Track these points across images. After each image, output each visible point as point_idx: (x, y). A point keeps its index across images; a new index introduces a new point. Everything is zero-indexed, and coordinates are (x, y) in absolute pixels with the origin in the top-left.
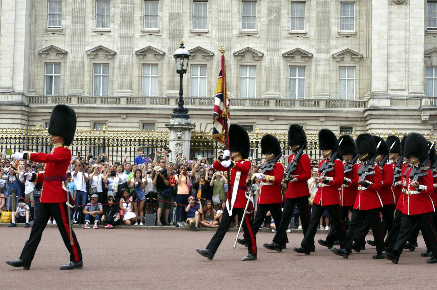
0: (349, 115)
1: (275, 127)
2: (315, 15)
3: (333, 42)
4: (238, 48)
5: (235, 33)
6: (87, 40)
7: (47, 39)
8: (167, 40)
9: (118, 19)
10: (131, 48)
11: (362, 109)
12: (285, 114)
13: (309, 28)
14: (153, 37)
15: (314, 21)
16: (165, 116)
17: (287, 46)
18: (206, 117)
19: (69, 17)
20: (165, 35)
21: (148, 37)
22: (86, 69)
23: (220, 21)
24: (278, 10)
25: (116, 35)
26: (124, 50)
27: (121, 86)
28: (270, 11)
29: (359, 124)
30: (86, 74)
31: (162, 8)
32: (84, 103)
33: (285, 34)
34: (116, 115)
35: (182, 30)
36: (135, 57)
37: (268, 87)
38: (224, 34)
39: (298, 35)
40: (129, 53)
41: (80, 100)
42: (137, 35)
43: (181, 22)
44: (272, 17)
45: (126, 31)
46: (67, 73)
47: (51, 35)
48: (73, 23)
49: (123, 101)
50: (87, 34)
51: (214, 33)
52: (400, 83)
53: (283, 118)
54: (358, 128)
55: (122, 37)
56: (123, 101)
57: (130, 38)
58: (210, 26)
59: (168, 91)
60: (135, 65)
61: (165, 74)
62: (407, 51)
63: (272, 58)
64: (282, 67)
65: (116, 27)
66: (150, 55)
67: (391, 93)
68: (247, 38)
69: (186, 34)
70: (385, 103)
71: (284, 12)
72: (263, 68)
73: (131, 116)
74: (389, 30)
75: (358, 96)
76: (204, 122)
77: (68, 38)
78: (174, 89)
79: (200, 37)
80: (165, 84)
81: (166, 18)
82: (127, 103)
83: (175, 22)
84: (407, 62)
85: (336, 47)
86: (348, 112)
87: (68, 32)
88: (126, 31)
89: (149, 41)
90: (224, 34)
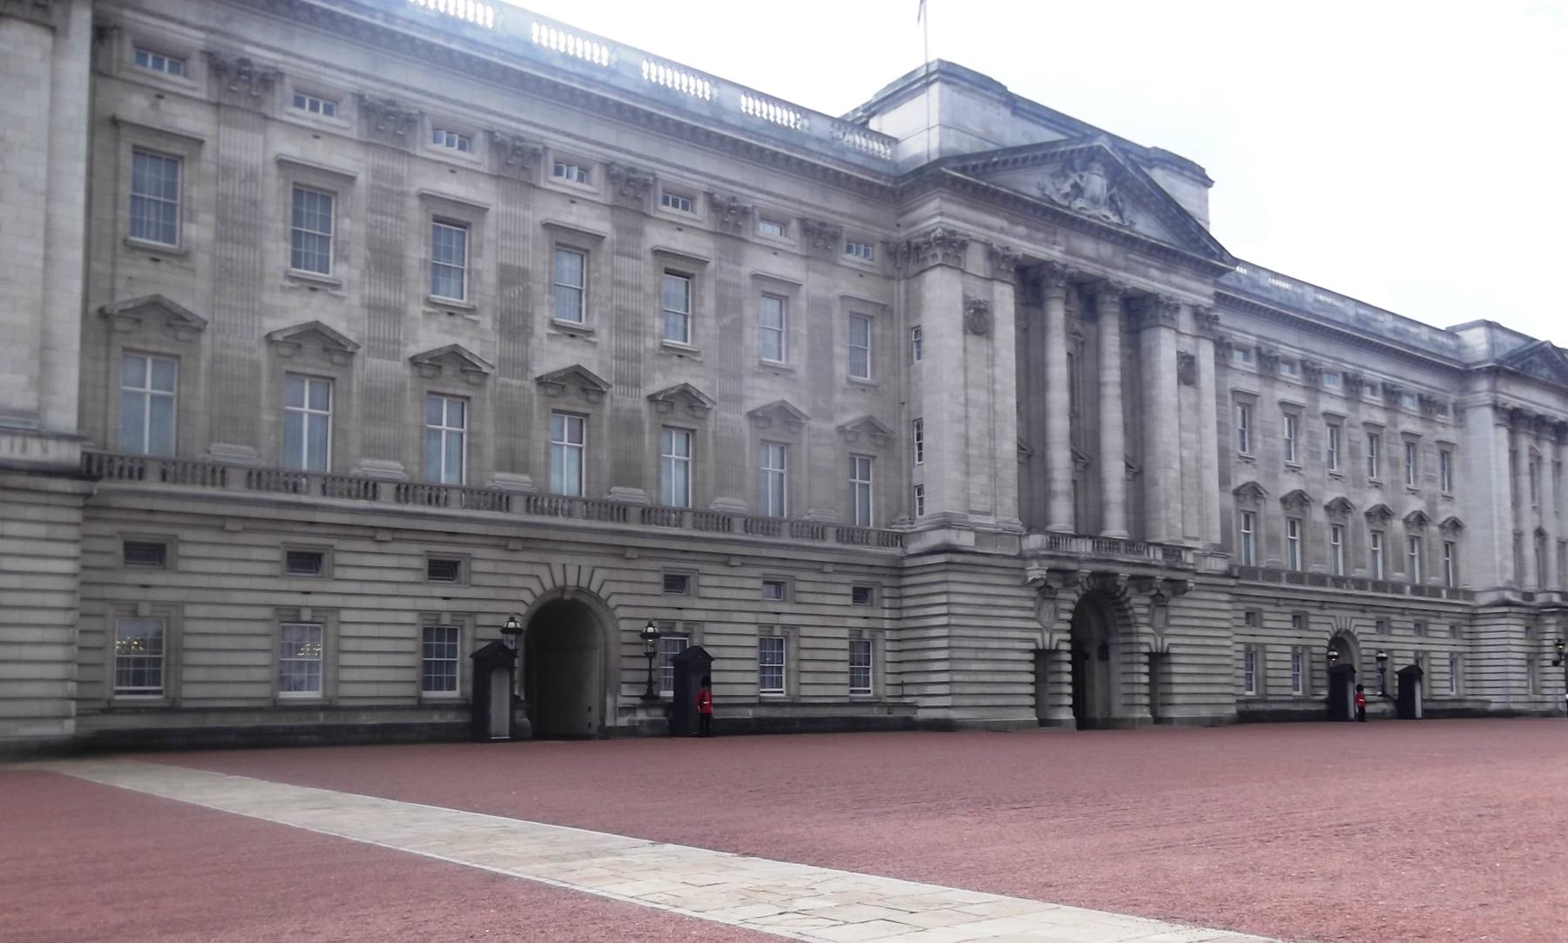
0: (878, 562)
1: (736, 583)
2: (804, 331)
3: (838, 398)
4: (658, 383)
5: (650, 343)
6: (267, 298)
7: (134, 272)
8: (494, 337)
9: (359, 252)
10: (398, 342)
11: (896, 551)
12: (764, 552)
13: (798, 359)
14: (458, 321)
15: (804, 342)
16: (495, 541)
17: (757, 394)
18: (594, 550)
19: (208, 218)
20: (487, 322)
21: (444, 319)
22: (265, 385)
23: (619, 308)
24: (738, 306)
25: (354, 299)
26: (389, 348)
27: (373, 449)
28: (722, 305)
29: (886, 582)
30: (264, 401)
31: (480, 247)
32: (268, 489)
33: (751, 363)
34: (360, 532)
35: (532, 315)
36: (408, 372)
37: (722, 488)
38: (628, 344)
39: (776, 371)
40: (394, 355)
41: (254, 477)
42: (416, 309)
43: (526, 294)
44: (726, 320)
45: (384, 293)
46: (202, 392)
47: (145, 263)
48: (221, 237)
49: (387, 491)
50: (268, 281)
51: (604, 336)
52: (982, 500)
53: (755, 561)
54: (886, 592)
55: (375, 308)
56: (387, 491)
57: (394, 313)
58: (596, 317)
59: (498, 475)
60: (409, 394)
61: (489, 429)
62: (992, 435)
63: (729, 416)
64: (748, 441)
65: (356, 274)
66: (449, 371)
67: (973, 519)
68: (675, 360)
69: (541, 329)
70: (966, 540)
71: (749, 311)
72: (711, 441)
73: (405, 536)
74: (966, 385)
75: (883, 520)
76: (586, 562)
77: (203, 284)
78: (513, 470)
79: (574, 341)
80: (490, 452)
81: (490, 278)
82: (398, 500)
83: (516, 291)
84: (992, 458)
85: (844, 410)
86: (875, 556)
87: (202, 261)
88: (384, 293)
89: (447, 332)
90: (628, 344)
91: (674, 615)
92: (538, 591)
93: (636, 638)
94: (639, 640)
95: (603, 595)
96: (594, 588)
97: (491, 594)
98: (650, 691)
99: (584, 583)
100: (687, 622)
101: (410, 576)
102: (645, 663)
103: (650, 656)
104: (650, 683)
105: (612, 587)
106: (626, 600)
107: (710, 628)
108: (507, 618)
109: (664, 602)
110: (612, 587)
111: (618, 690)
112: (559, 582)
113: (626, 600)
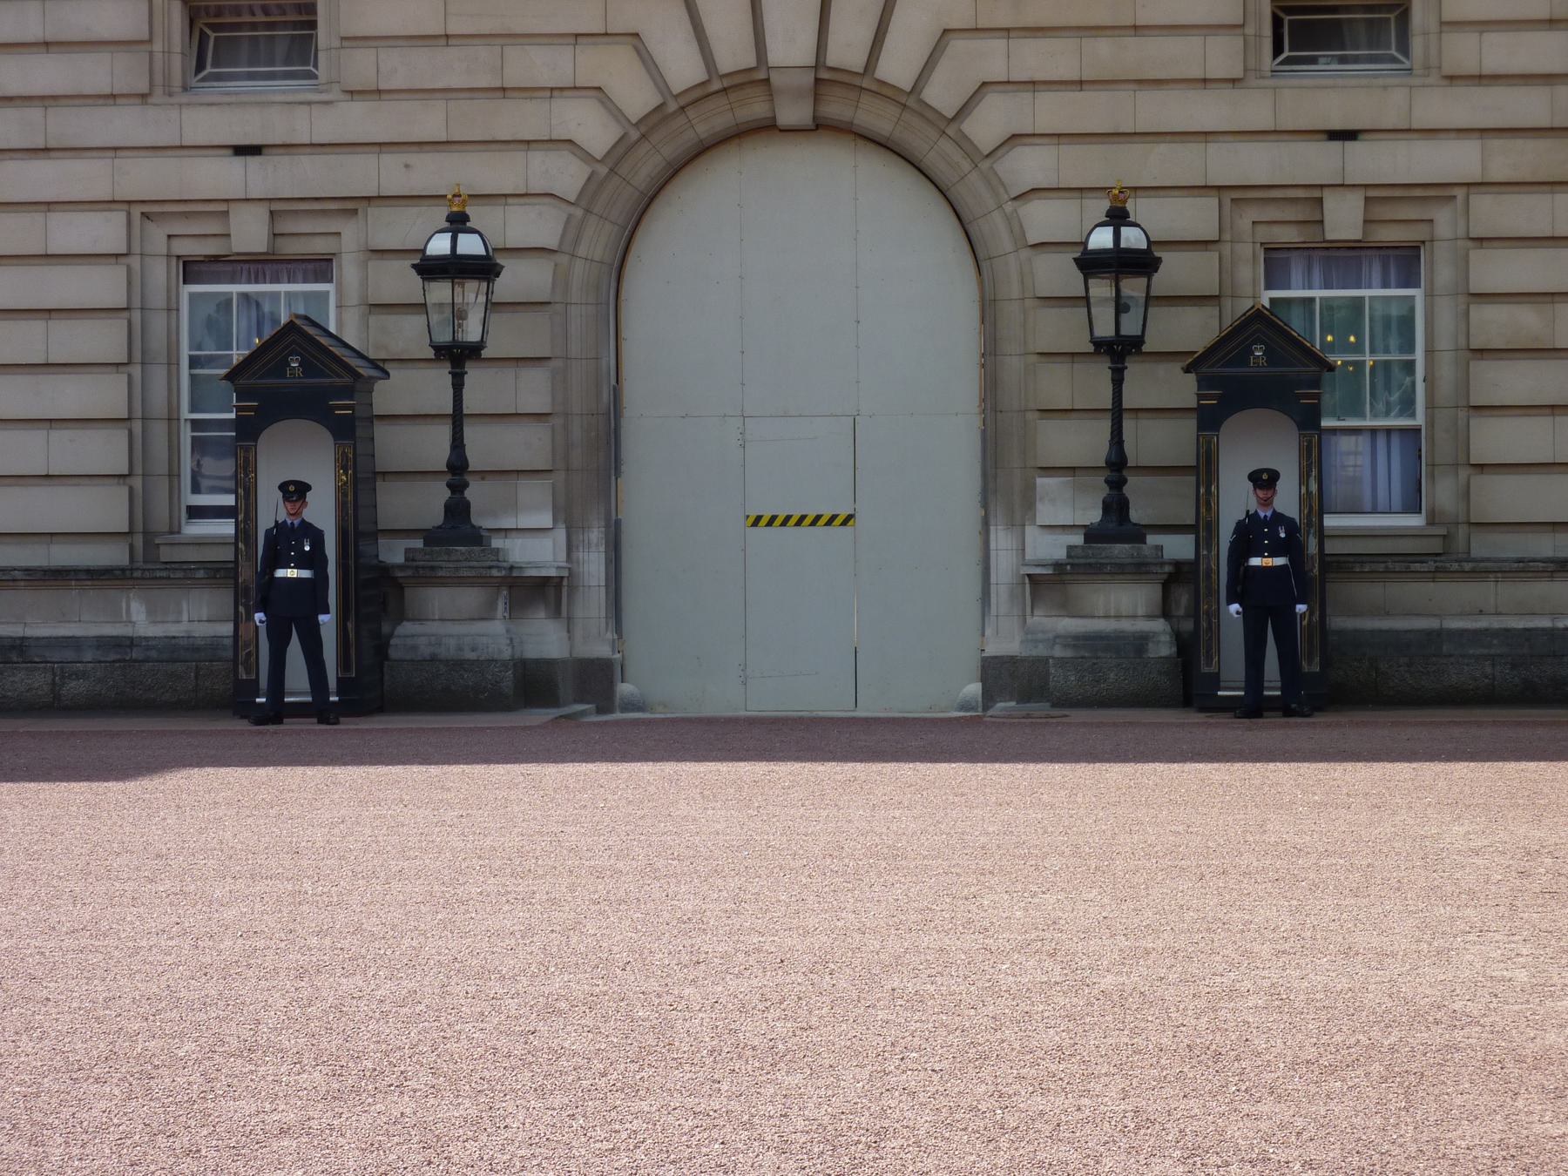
91: (1318, 162)
92: (637, 98)
93: (1060, 274)
94: (1072, 281)
95: (942, 94)
96: (897, 67)
97: (429, 122)
98: (1116, 507)
99: (847, 49)
100: (1377, 196)
101: (94, 73)
102: (1095, 383)
103: (1119, 351)
104: (1117, 466)
105: (993, 59)
106: (1051, 112)
107: (1492, 213)
108: (440, 214)
109: (1254, 110)
110: (993, 59)
111: (1029, 501)
112: (733, 53)
113: (1051, 112)
